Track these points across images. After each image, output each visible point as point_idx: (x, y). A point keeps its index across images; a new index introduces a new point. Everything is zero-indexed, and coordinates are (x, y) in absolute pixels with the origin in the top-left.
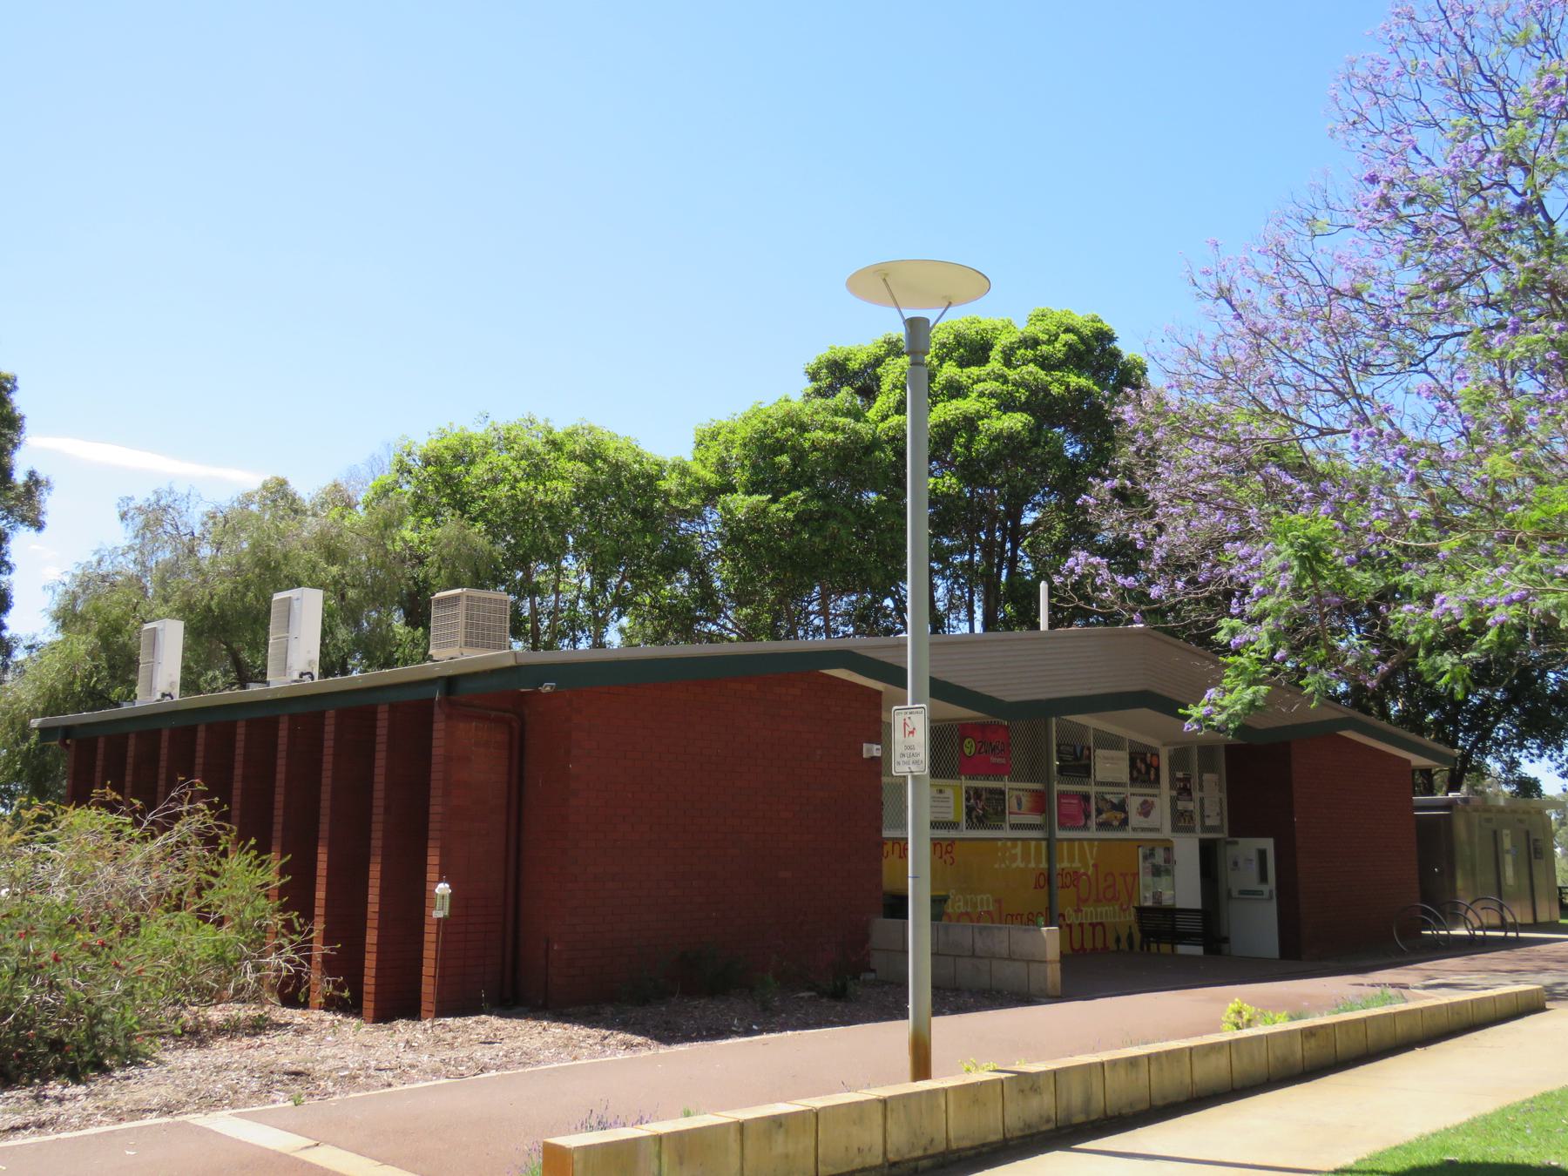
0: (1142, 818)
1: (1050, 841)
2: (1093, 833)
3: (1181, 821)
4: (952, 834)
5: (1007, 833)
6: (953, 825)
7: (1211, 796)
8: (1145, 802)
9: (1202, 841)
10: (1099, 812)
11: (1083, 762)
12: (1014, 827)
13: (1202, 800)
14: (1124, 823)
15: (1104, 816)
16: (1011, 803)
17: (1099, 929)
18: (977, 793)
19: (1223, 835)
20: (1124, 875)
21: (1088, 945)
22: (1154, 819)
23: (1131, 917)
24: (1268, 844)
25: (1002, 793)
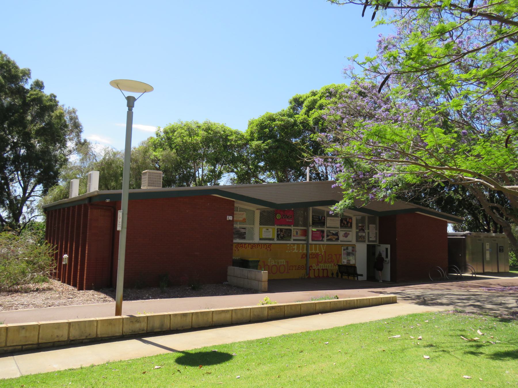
0: (344, 238)
1: (307, 244)
2: (325, 242)
3: (360, 239)
4: (271, 242)
5: (292, 242)
6: (272, 239)
7: (372, 232)
8: (346, 233)
9: (368, 245)
10: (328, 236)
11: (322, 221)
12: (294, 240)
13: (368, 233)
14: (337, 239)
15: (330, 237)
16: (294, 233)
17: (325, 271)
18: (281, 230)
19: (377, 243)
20: (336, 255)
21: (321, 275)
22: (349, 238)
23: (337, 267)
24: (388, 246)
25: (291, 230)
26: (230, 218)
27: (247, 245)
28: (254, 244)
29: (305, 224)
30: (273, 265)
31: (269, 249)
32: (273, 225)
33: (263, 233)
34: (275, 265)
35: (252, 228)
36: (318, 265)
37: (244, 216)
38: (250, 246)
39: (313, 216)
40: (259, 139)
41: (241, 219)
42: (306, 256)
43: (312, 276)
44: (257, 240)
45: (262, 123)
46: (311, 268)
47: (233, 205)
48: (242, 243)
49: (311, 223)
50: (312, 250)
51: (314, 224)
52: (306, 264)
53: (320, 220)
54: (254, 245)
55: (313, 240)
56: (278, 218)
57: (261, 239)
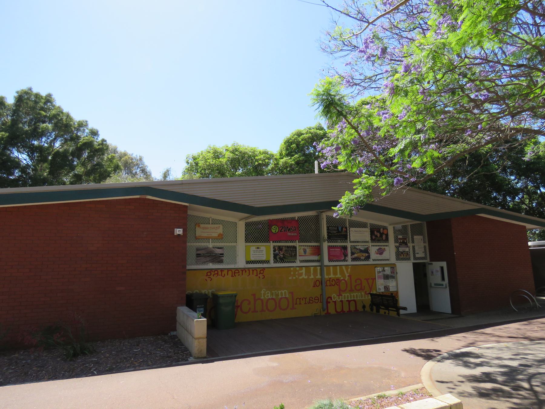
0: (378, 255)
1: (322, 267)
2: (350, 262)
3: (401, 256)
4: (265, 265)
5: (298, 264)
6: (268, 262)
7: (419, 246)
8: (380, 249)
9: (414, 265)
10: (353, 254)
11: (343, 233)
12: (302, 261)
13: (414, 247)
14: (368, 258)
15: (356, 255)
16: (300, 251)
17: (352, 303)
18: (280, 248)
19: (428, 260)
20: (367, 280)
21: (346, 309)
22: (385, 255)
23: (370, 297)
24: (444, 264)
25: (295, 247)
26: (179, 231)
27: (226, 272)
28: (237, 269)
29: (317, 238)
30: (269, 299)
31: (261, 276)
32: (268, 241)
33: (252, 253)
34: (272, 299)
35: (235, 247)
36: (340, 295)
37: (220, 231)
38: (230, 272)
39: (328, 227)
40: (287, 155)
41: (216, 235)
42: (320, 283)
43: (332, 311)
44: (241, 264)
45: (290, 139)
46: (329, 300)
47: (186, 212)
48: (216, 270)
49: (326, 236)
50: (329, 274)
51: (331, 237)
52: (321, 295)
53: (338, 232)
54: (236, 272)
55: (330, 260)
56: (274, 231)
57: (248, 262)
